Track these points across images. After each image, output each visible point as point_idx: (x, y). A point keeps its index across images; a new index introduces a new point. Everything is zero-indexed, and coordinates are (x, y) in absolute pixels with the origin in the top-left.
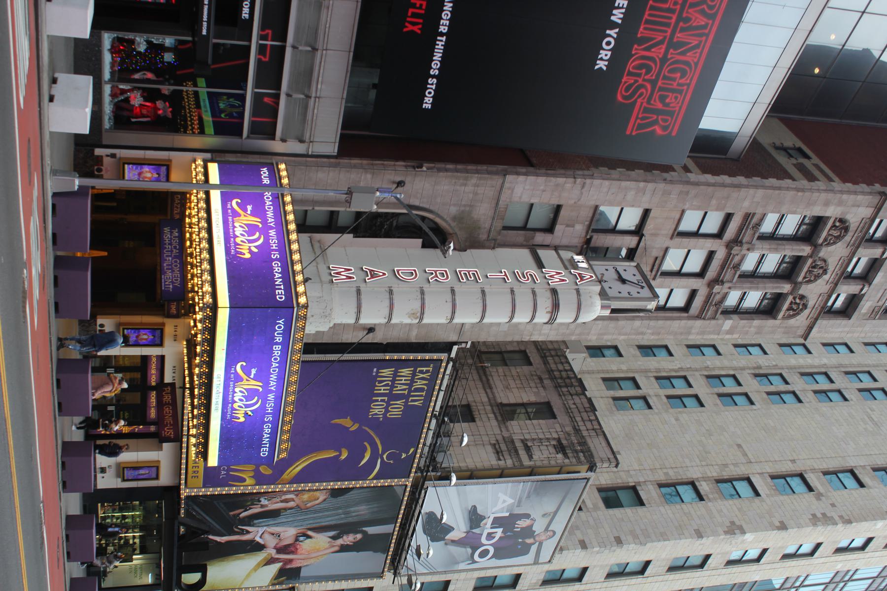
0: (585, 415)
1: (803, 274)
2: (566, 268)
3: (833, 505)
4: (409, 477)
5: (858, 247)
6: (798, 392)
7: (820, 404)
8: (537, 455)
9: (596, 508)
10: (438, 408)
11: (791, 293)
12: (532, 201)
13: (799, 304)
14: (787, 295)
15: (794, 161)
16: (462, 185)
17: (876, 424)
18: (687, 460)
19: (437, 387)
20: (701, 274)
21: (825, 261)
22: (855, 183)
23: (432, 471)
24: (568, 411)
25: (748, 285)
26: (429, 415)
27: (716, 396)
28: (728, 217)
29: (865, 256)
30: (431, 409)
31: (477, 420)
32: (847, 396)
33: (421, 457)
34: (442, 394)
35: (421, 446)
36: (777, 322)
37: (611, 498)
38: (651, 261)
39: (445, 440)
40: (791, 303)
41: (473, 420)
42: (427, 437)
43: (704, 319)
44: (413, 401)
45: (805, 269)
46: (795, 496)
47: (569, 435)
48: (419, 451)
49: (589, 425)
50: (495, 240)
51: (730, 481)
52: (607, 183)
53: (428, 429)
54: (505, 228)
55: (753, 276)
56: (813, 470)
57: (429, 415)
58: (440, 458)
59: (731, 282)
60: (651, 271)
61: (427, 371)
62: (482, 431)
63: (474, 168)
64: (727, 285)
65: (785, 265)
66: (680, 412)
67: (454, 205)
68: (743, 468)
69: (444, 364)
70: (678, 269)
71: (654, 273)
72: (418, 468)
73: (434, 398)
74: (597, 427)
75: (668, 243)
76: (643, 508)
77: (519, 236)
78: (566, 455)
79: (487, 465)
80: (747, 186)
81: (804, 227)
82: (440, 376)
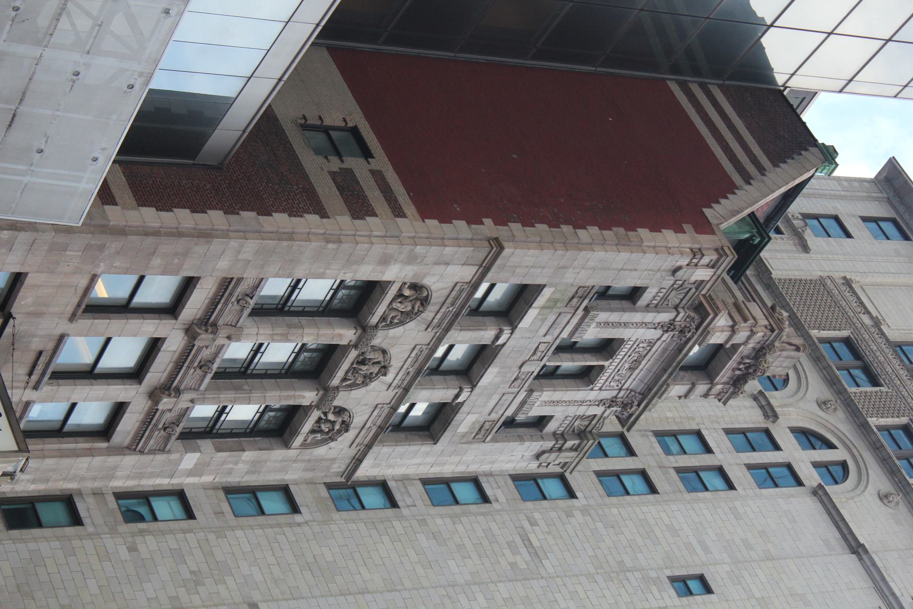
1: (340, 374)
5: (447, 330)
6: (392, 484)
7: (434, 510)
11: (318, 407)
14: (345, 349)
15: (335, 164)
17: (536, 554)
20: (136, 374)
21: (384, 352)
22: (445, 219)
25: (231, 395)
27: (221, 494)
28: (188, 285)
29: (461, 342)
32: (489, 492)
36: (291, 453)
38: (30, 357)
40: (319, 420)
43: (141, 452)
45: (345, 365)
55: (243, 374)
59: (196, 389)
60: (30, 374)
65: (272, 414)
66: (141, 532)
70: (61, 416)
71: (34, 378)
75: (63, 326)
81: (342, 293)
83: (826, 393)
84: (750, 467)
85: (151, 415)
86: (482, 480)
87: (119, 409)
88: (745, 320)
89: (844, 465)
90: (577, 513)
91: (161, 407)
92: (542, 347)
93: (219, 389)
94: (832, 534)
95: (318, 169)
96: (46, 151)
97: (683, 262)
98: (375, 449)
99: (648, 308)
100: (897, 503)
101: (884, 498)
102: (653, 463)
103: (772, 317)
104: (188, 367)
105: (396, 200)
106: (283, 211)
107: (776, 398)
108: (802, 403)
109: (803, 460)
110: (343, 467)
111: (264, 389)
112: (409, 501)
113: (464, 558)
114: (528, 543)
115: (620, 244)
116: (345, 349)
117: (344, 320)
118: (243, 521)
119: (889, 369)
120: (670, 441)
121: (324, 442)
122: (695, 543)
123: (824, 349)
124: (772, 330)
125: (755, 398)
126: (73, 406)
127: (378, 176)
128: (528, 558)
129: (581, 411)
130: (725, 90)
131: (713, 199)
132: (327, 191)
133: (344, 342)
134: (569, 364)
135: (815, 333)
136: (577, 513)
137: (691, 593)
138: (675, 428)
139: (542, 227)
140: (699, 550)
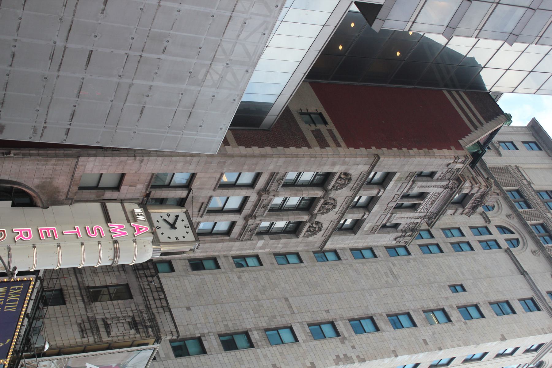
0: (156, 294)
1: (317, 209)
2: (128, 221)
3: (353, 347)
4: (7, 358)
6: (338, 251)
7: (355, 261)
8: (115, 332)
9: (167, 358)
10: (29, 311)
11: (309, 222)
12: (101, 173)
13: (315, 228)
15: (313, 127)
16: (43, 165)
17: (395, 277)
18: (244, 314)
19: (28, 298)
20: (239, 211)
21: (334, 200)
22: (357, 147)
23: (27, 351)
24: (142, 291)
25: (275, 218)
26: (22, 316)
27: (273, 256)
28: (258, 176)
30: (24, 309)
31: (67, 302)
32: (376, 253)
33: (16, 344)
34: (32, 302)
35: (16, 337)
36: (299, 240)
37: (180, 349)
38: (199, 205)
39: (39, 323)
40: (310, 227)
41: (64, 303)
42: (21, 329)
43: (242, 240)
44: (7, 308)
45: (319, 205)
46: (326, 341)
47: (141, 312)
48: (15, 340)
49: (158, 302)
50: (72, 199)
51: (277, 329)
52: (160, 159)
53: (22, 325)
54: (81, 188)
55: (280, 210)
56: (342, 319)
57: (22, 316)
58: (33, 339)
60: (199, 212)
61: (19, 289)
62: (71, 314)
63: (54, 152)
64: (258, 219)
67: (37, 178)
68: (287, 319)
69: (33, 283)
70: (211, 227)
71: (201, 213)
72: (15, 351)
73: (25, 306)
74: (165, 304)
76: (206, 356)
77: (92, 194)
78: (137, 330)
79: (72, 342)
80: (272, 156)
81: (317, 177)
82: (30, 291)
83: (510, 212)
84: (480, 241)
85: (245, 226)
86: (374, 249)
87: (233, 224)
88: (477, 184)
89: (517, 240)
90: (411, 261)
91: (249, 223)
92: (396, 196)
93: (271, 216)
94: (513, 267)
95: (307, 129)
96: (203, 126)
97: (451, 161)
98: (332, 237)
99: (437, 180)
100: (539, 255)
101: (534, 252)
102: (441, 241)
103: (487, 182)
104: (259, 207)
105: (337, 140)
106: (294, 146)
107: (489, 214)
108: (500, 216)
109: (501, 238)
110: (320, 245)
111: (288, 215)
112: (345, 258)
113: (367, 279)
114: (392, 273)
115: (426, 155)
116: (319, 199)
117: (318, 188)
118: (281, 266)
119: (534, 202)
120: (447, 232)
121: (312, 235)
122: (458, 271)
123: (508, 194)
124: (488, 187)
125: (481, 214)
126: (216, 223)
127: (330, 131)
128: (392, 279)
129: (412, 221)
130: (466, 93)
131: (462, 136)
132: (310, 137)
133: (319, 196)
134: (407, 202)
135: (504, 188)
136: (411, 261)
137: (457, 292)
138: (449, 227)
139: (395, 149)
140: (460, 274)
